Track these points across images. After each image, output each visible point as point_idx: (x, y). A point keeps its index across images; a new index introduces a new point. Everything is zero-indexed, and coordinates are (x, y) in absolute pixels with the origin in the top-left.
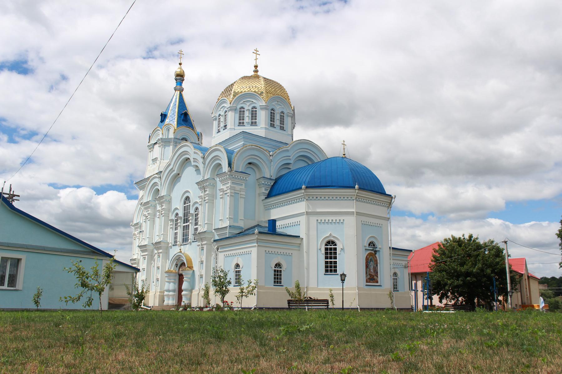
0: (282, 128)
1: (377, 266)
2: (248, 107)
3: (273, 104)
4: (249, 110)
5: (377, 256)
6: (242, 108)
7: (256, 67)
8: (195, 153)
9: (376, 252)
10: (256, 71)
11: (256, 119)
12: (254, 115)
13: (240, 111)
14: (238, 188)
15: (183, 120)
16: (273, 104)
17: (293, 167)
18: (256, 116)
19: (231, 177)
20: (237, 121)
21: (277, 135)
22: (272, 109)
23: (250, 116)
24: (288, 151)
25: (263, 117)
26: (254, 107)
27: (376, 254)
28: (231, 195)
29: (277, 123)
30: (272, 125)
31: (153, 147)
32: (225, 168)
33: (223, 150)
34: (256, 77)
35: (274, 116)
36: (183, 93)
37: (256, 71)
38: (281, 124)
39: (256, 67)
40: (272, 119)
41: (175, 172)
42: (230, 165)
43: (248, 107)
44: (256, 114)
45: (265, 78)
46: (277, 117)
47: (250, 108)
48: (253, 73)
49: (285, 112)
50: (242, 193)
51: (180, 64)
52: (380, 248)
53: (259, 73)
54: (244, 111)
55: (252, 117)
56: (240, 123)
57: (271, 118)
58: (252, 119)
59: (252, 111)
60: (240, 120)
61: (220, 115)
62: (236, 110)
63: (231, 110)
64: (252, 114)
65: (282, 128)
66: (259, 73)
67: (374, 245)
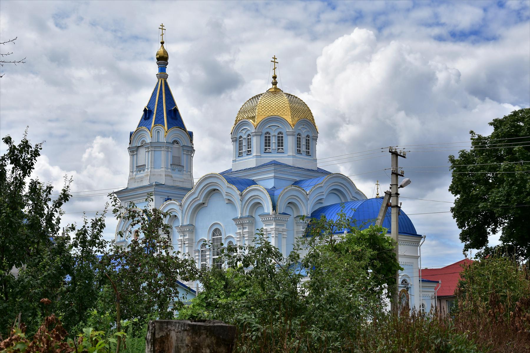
0: (308, 153)
1: (408, 301)
2: (274, 133)
3: (299, 128)
4: (275, 136)
5: (409, 292)
6: (268, 133)
7: (275, 77)
8: (228, 187)
9: (408, 289)
10: (275, 84)
11: (282, 146)
12: (280, 143)
13: (266, 137)
14: (281, 228)
15: (172, 118)
16: (299, 128)
17: (326, 204)
18: (282, 143)
19: (276, 220)
20: (263, 147)
21: (302, 162)
22: (299, 134)
23: (277, 142)
24: (322, 187)
25: (290, 142)
26: (280, 133)
27: (408, 291)
28: (276, 237)
29: (303, 148)
30: (299, 152)
31: (137, 150)
32: (268, 208)
33: (266, 192)
34: (276, 91)
35: (300, 141)
36: (168, 81)
37: (275, 84)
38: (306, 149)
39: (275, 77)
40: (299, 145)
41: (201, 202)
42: (274, 208)
43: (274, 133)
44: (282, 140)
45: (287, 94)
46: (303, 142)
47: (276, 134)
48: (271, 86)
49: (311, 135)
50: (285, 233)
51: (162, 43)
52: (411, 285)
53: (278, 86)
54: (269, 137)
55: (279, 143)
56: (266, 149)
57: (298, 144)
58: (279, 146)
59: (279, 137)
60: (266, 146)
61: (241, 137)
62: (261, 135)
63: (256, 135)
64: (279, 140)
65: (308, 153)
66: (278, 86)
67: (406, 282)
